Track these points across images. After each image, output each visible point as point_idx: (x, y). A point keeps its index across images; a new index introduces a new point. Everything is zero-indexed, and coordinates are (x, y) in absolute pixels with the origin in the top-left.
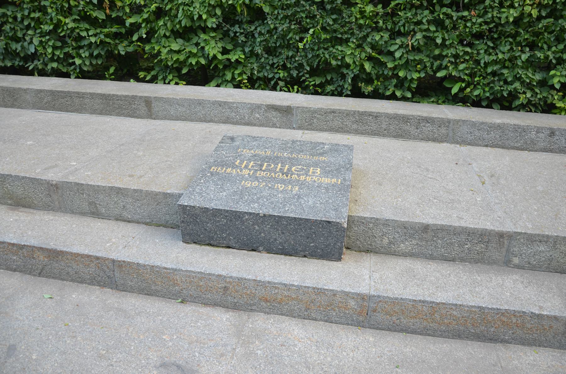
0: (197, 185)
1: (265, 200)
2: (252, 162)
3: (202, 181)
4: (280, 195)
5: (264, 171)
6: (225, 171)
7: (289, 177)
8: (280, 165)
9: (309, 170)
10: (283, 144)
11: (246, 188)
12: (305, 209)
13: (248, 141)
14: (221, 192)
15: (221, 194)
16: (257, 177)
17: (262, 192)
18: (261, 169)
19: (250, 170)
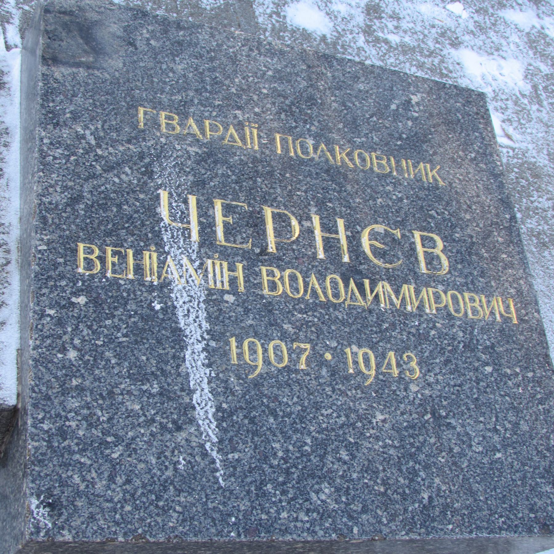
0: (65, 392)
1: (344, 455)
2: (218, 204)
3: (72, 355)
4: (380, 417)
5: (277, 261)
6: (139, 269)
7: (370, 297)
8: (316, 220)
9: (413, 249)
10: (279, 77)
11: (257, 384)
12: (476, 486)
13: (155, 53)
14: (179, 428)
15: (181, 436)
16: (269, 307)
17: (317, 407)
18: (264, 251)
19: (225, 254)
